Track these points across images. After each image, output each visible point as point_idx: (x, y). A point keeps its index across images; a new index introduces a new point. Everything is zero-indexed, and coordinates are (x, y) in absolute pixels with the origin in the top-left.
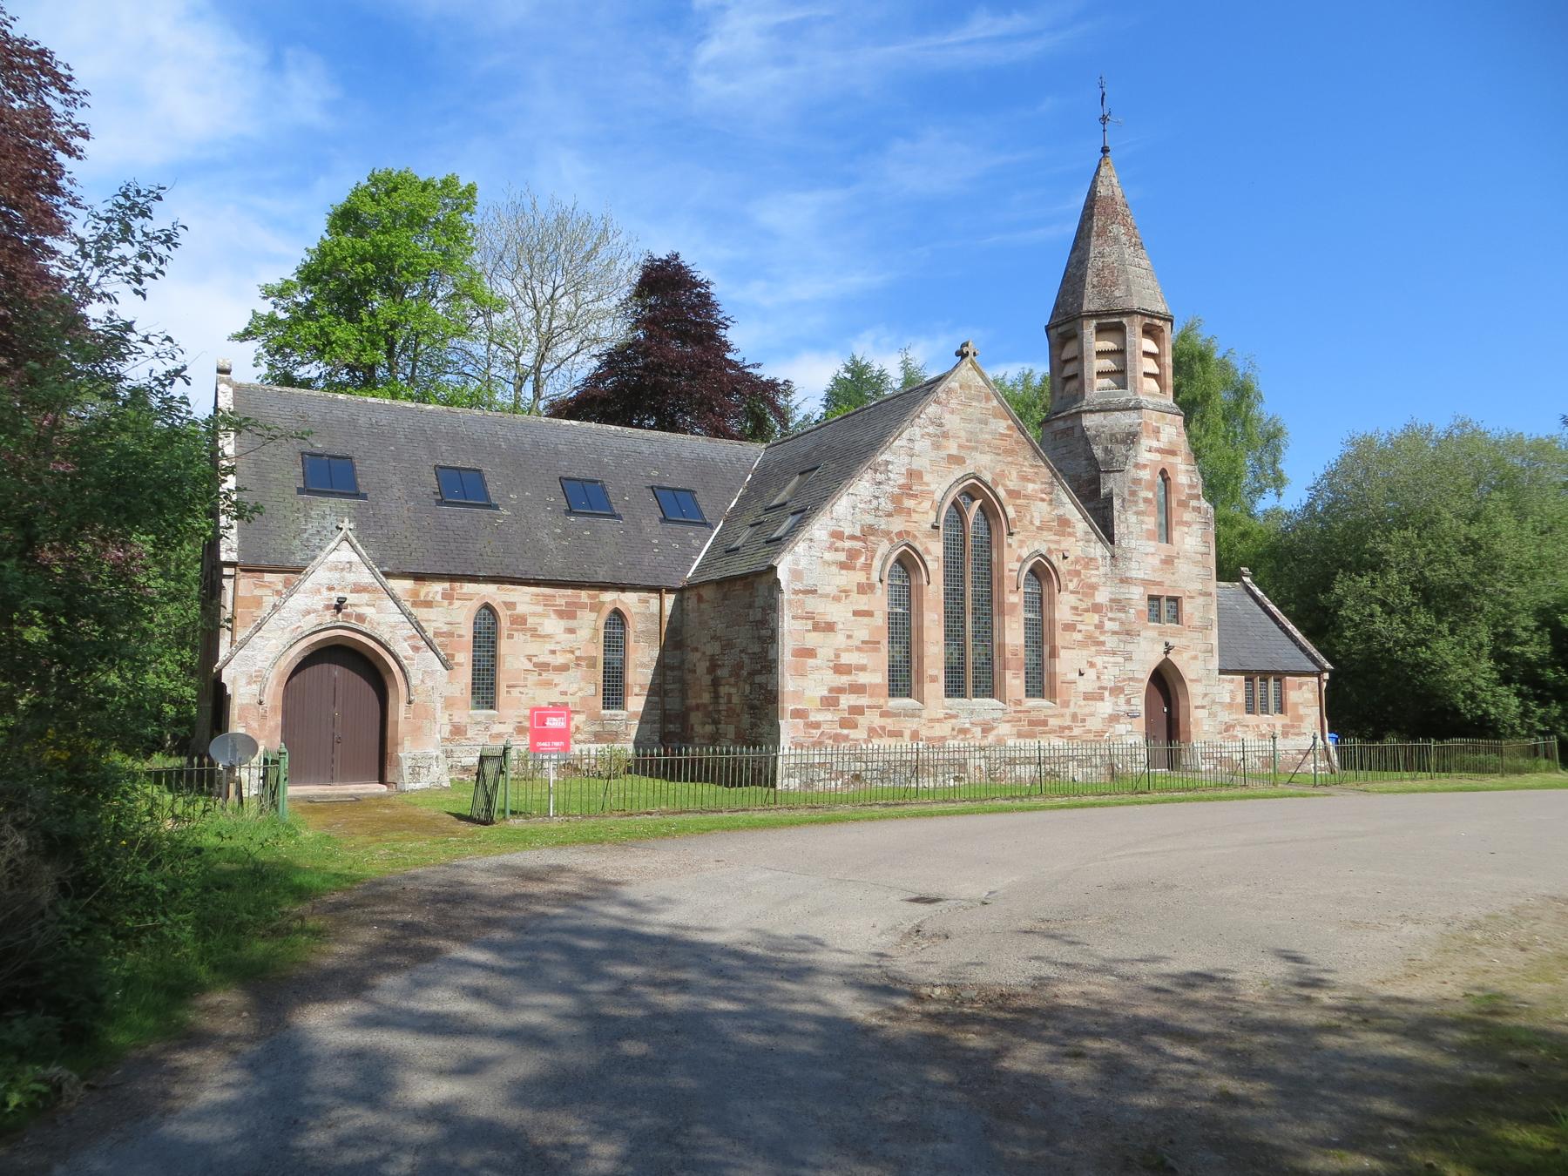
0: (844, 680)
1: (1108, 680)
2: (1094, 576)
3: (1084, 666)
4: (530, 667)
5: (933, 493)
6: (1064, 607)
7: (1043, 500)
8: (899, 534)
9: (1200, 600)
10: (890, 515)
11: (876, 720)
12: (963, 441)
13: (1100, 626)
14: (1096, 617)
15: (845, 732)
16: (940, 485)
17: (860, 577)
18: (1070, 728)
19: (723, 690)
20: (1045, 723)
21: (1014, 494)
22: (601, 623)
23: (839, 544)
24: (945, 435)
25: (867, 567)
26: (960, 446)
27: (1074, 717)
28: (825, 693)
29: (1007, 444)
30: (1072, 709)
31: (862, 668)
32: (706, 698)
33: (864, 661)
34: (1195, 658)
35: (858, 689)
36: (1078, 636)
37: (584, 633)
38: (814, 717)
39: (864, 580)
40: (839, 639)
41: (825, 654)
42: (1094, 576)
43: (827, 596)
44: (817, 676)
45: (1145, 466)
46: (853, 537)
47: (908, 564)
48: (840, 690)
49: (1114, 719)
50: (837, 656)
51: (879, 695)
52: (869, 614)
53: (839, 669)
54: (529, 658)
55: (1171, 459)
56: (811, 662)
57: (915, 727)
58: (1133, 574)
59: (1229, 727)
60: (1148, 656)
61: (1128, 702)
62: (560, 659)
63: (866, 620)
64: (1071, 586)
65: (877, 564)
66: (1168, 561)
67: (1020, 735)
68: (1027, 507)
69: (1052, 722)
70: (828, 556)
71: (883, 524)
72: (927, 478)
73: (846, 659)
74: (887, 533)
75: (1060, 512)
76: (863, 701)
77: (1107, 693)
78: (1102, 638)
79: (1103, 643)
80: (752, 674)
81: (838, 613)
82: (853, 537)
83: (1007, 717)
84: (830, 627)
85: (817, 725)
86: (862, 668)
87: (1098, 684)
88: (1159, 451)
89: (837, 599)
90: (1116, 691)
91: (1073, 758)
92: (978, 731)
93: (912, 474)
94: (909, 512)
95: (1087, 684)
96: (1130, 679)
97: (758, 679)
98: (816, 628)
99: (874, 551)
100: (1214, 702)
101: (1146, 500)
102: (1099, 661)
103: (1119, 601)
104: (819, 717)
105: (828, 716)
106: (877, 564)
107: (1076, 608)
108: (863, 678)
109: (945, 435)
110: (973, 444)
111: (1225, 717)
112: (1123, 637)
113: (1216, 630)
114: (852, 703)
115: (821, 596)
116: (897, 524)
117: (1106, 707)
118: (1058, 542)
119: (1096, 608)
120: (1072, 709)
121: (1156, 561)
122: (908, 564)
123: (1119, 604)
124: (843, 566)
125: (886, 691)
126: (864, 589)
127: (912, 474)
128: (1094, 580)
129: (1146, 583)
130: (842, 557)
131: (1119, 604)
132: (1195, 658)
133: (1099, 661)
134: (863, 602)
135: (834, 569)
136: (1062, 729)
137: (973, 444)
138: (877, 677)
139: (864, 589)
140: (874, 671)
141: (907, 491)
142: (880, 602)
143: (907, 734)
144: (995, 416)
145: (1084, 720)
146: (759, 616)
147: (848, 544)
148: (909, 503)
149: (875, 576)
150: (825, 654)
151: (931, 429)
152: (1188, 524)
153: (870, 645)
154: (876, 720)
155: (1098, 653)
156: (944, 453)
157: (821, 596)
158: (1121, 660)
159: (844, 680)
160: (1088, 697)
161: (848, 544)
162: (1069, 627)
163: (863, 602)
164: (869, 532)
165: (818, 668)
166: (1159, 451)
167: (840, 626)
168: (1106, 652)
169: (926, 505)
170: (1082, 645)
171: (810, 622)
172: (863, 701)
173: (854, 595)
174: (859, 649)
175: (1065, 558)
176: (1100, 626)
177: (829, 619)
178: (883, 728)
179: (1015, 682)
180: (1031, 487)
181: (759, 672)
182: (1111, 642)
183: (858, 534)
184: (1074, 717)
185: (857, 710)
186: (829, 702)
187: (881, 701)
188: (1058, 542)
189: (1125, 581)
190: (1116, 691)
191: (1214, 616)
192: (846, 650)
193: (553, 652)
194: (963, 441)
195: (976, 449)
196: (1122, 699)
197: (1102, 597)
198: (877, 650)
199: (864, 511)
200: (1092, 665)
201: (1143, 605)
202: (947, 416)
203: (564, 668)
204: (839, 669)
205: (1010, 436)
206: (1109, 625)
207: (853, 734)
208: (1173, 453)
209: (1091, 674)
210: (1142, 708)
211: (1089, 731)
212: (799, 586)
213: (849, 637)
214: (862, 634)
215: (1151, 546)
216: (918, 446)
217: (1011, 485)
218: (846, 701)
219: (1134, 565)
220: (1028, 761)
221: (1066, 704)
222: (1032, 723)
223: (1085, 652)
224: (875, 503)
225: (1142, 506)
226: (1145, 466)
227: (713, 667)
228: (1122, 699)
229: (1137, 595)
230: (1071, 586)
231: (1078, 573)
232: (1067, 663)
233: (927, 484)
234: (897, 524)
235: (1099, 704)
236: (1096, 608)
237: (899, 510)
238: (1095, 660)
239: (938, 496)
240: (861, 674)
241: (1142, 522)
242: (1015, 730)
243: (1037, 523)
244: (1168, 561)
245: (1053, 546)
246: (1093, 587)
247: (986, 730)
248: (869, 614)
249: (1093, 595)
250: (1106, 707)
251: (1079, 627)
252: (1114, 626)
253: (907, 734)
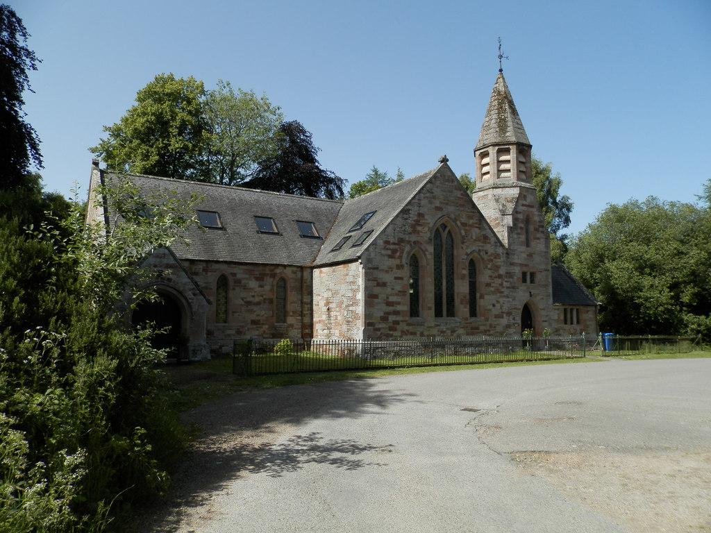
0: (391, 309)
1: (505, 308)
3: (495, 302)
4: (243, 303)
5: (429, 224)
6: (484, 277)
7: (477, 227)
8: (414, 242)
9: (544, 273)
13: (501, 285)
14: (500, 280)
15: (391, 332)
17: (397, 262)
18: (489, 331)
19: (332, 314)
20: (478, 328)
21: (464, 224)
22: (275, 283)
23: (388, 246)
24: (434, 197)
25: (400, 257)
26: (441, 203)
27: (491, 326)
28: (382, 315)
30: (489, 322)
31: (399, 303)
32: (324, 317)
33: (400, 300)
35: (397, 313)
37: (267, 288)
38: (377, 326)
40: (389, 290)
41: (382, 296)
42: (499, 262)
43: (383, 270)
46: (394, 244)
48: (388, 313)
49: (508, 326)
50: (388, 298)
52: (401, 278)
53: (389, 304)
54: (242, 299)
55: (531, 209)
56: (376, 300)
57: (421, 330)
58: (516, 261)
59: (557, 330)
60: (522, 296)
61: (514, 319)
62: (257, 299)
63: (400, 281)
64: (489, 266)
65: (405, 255)
66: (530, 255)
67: (468, 334)
69: (482, 328)
70: (383, 252)
73: (392, 299)
74: (409, 242)
75: (484, 233)
76: (399, 318)
79: (502, 292)
80: (348, 306)
81: (388, 278)
82: (394, 244)
84: (384, 285)
85: (379, 329)
86: (399, 303)
87: (501, 311)
89: (387, 272)
90: (509, 314)
93: (420, 215)
95: (496, 311)
97: (351, 308)
98: (378, 285)
99: (403, 250)
101: (521, 228)
102: (501, 300)
105: (384, 325)
106: (405, 255)
107: (491, 277)
108: (399, 308)
109: (434, 197)
111: (555, 325)
113: (551, 287)
114: (394, 319)
117: (504, 321)
118: (482, 246)
119: (500, 276)
120: (489, 322)
121: (524, 255)
123: (510, 275)
124: (390, 257)
125: (409, 314)
126: (400, 267)
127: (420, 215)
128: (499, 264)
129: (521, 265)
130: (389, 252)
131: (510, 275)
133: (501, 300)
134: (399, 273)
135: (386, 258)
136: (486, 331)
138: (405, 307)
139: (400, 267)
141: (417, 223)
143: (418, 333)
144: (456, 189)
145: (495, 327)
147: (392, 247)
148: (419, 228)
149: (404, 261)
150: (382, 296)
151: (428, 195)
152: (539, 239)
153: (402, 293)
155: (501, 297)
156: (433, 206)
159: (391, 309)
160: (497, 316)
161: (392, 247)
162: (488, 285)
163: (399, 273)
164: (401, 241)
167: (389, 284)
168: (504, 296)
169: (426, 229)
170: (494, 293)
171: (376, 282)
172: (399, 318)
175: (487, 253)
176: (501, 285)
177: (384, 281)
179: (463, 310)
180: (471, 221)
181: (352, 305)
182: (506, 292)
183: (396, 242)
184: (491, 326)
185: (397, 323)
186: (384, 319)
187: (407, 319)
188: (482, 246)
189: (512, 264)
190: (509, 314)
191: (550, 280)
192: (391, 295)
193: (253, 296)
195: (447, 204)
196: (511, 318)
197: (502, 271)
199: (399, 232)
201: (520, 275)
202: (435, 189)
203: (258, 304)
204: (389, 304)
206: (505, 284)
207: (395, 334)
209: (498, 306)
210: (520, 322)
211: (497, 332)
213: (393, 289)
215: (523, 248)
216: (423, 202)
217: (463, 221)
218: (392, 318)
219: (516, 257)
221: (487, 320)
222: (472, 328)
224: (403, 228)
225: (519, 231)
226: (520, 213)
227: (328, 303)
228: (511, 318)
229: (517, 271)
230: (489, 266)
231: (492, 261)
232: (485, 302)
234: (414, 238)
235: (501, 320)
236: (500, 276)
237: (415, 231)
239: (431, 225)
240: (398, 306)
241: (519, 238)
243: (474, 238)
246: (498, 267)
247: (453, 331)
248: (401, 278)
250: (504, 321)
252: (508, 285)
253: (418, 333)
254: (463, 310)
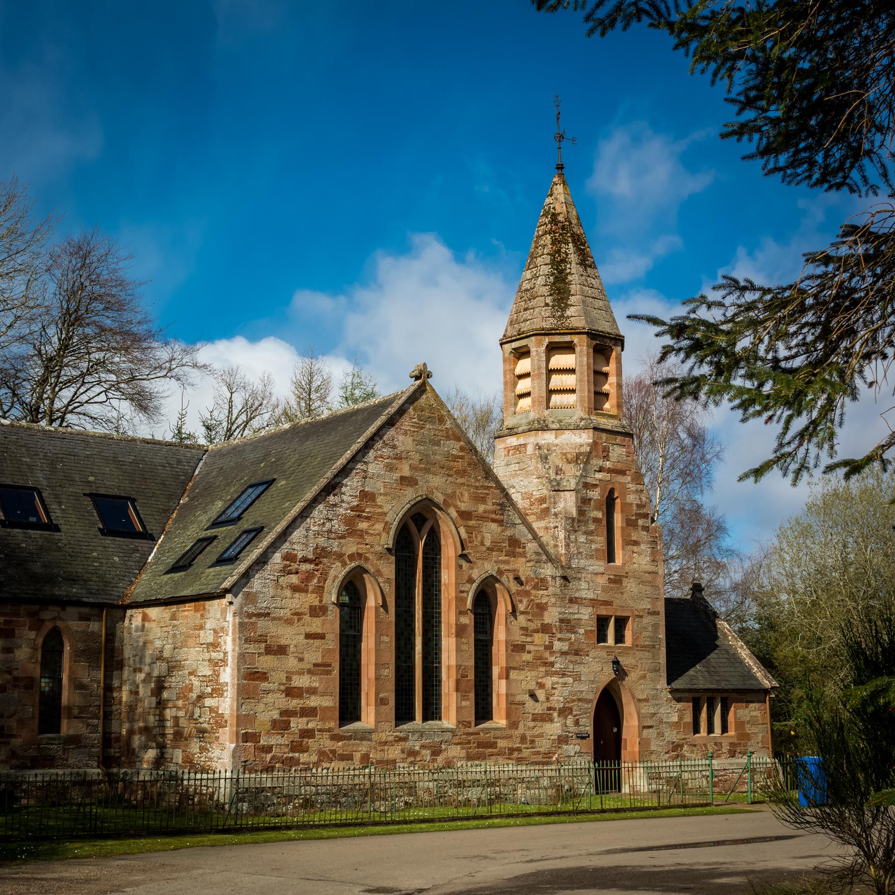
0: (294, 703)
1: (557, 700)
2: (542, 596)
7: (493, 521)
8: (352, 557)
9: (647, 620)
10: (343, 537)
11: (327, 744)
12: (416, 462)
13: (549, 647)
14: (547, 637)
16: (394, 509)
17: (312, 599)
18: (519, 750)
20: (493, 745)
25: (320, 590)
27: (523, 738)
29: (459, 465)
31: (312, 691)
33: (316, 684)
34: (643, 677)
36: (527, 657)
39: (317, 603)
40: (291, 662)
42: (542, 596)
43: (279, 619)
44: (270, 698)
45: (595, 486)
46: (305, 560)
47: (352, 591)
49: (562, 740)
50: (289, 679)
51: (330, 719)
52: (321, 636)
53: (291, 692)
56: (264, 685)
61: (577, 723)
63: (317, 642)
66: (617, 580)
67: (469, 758)
68: (477, 528)
69: (502, 744)
71: (335, 546)
72: (380, 500)
74: (340, 556)
77: (555, 714)
78: (552, 659)
79: (552, 664)
82: (305, 560)
83: (456, 740)
84: (282, 650)
85: (268, 749)
86: (312, 691)
88: (609, 471)
89: (289, 622)
90: (564, 712)
91: (522, 781)
92: (427, 753)
93: (365, 496)
94: (361, 534)
96: (580, 700)
98: (269, 651)
100: (661, 722)
101: (596, 520)
102: (548, 681)
103: (568, 621)
104: (273, 741)
108: (313, 702)
109: (398, 458)
110: (427, 465)
112: (574, 658)
115: (274, 619)
116: (351, 547)
117: (554, 728)
119: (545, 629)
120: (521, 730)
121: (602, 581)
122: (352, 591)
123: (567, 624)
126: (317, 611)
127: (365, 496)
129: (594, 603)
130: (294, 579)
132: (643, 677)
134: (316, 625)
136: (512, 750)
137: (427, 465)
138: (330, 702)
139: (317, 611)
140: (323, 694)
142: (330, 624)
143: (357, 756)
146: (210, 639)
148: (363, 525)
153: (320, 668)
154: (327, 744)
155: (547, 674)
156: (396, 476)
157: (274, 619)
158: (570, 680)
159: (294, 703)
163: (316, 625)
165: (268, 692)
166: (609, 471)
167: (292, 649)
173: (307, 618)
174: (310, 672)
177: (283, 642)
178: (333, 752)
181: (211, 695)
185: (307, 734)
186: (280, 726)
190: (564, 712)
192: (301, 673)
194: (416, 462)
196: (570, 721)
197: (551, 616)
198: (328, 673)
200: (541, 686)
202: (401, 438)
204: (291, 692)
205: (462, 457)
206: (557, 645)
207: (304, 757)
208: (622, 473)
210: (590, 729)
211: (538, 753)
212: (252, 610)
213: (301, 660)
214: (313, 656)
217: (463, 507)
218: (297, 724)
219: (584, 585)
220: (476, 783)
222: (480, 745)
223: (534, 673)
224: (328, 525)
226: (595, 486)
228: (570, 721)
229: (586, 615)
233: (380, 507)
234: (351, 547)
236: (545, 629)
237: (352, 532)
238: (544, 681)
240: (313, 698)
242: (463, 753)
244: (617, 580)
245: (504, 567)
247: (436, 753)
248: (321, 636)
249: (542, 615)
250: (554, 728)
251: (528, 647)
253: (357, 756)
254: (453, 705)
